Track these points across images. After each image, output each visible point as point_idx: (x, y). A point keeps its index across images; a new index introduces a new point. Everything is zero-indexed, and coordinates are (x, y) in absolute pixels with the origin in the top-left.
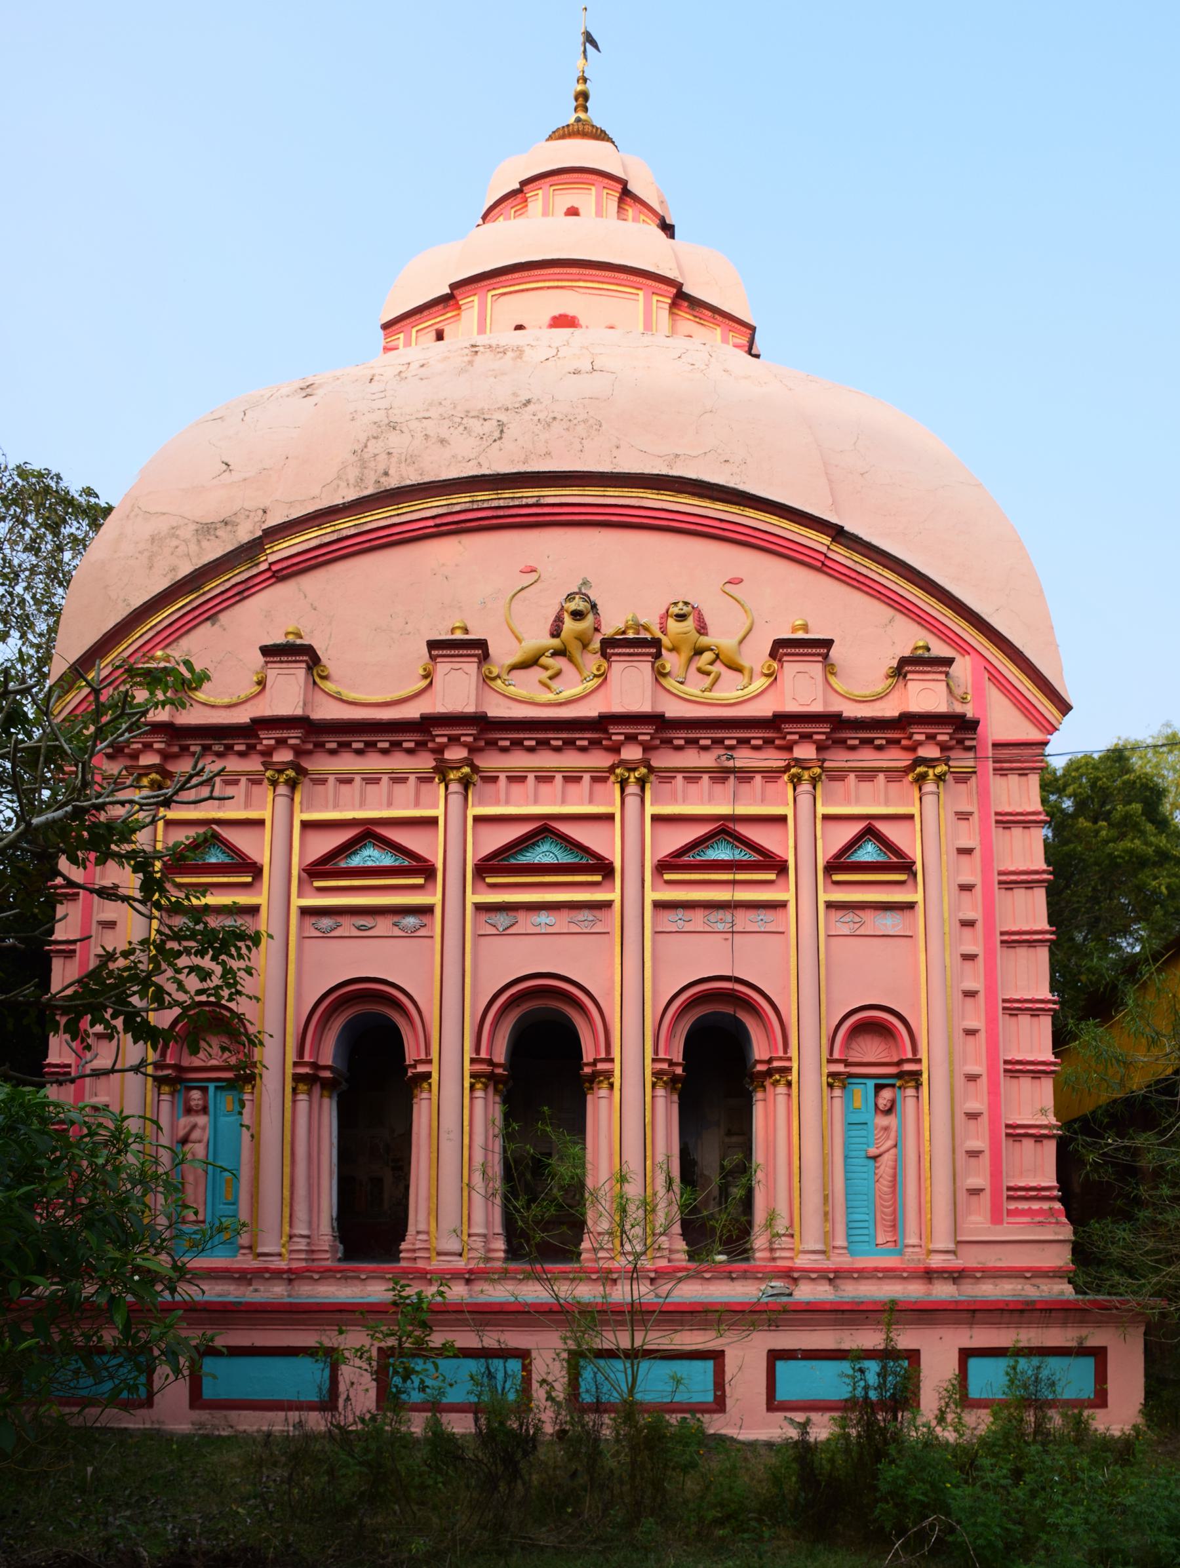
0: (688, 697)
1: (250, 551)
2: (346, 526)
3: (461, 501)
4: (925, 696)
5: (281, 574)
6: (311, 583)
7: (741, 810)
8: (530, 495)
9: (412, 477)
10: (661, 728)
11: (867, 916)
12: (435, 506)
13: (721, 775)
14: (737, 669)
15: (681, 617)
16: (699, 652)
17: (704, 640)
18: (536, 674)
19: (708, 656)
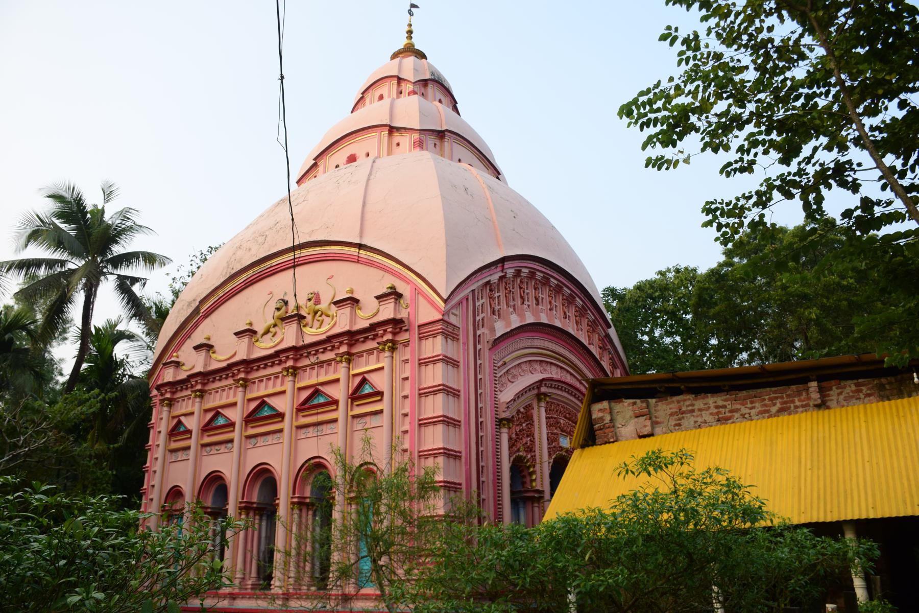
0: (313, 334)
1: (197, 311)
2: (221, 293)
3: (250, 273)
4: (387, 311)
5: (207, 315)
6: (214, 316)
7: (322, 379)
8: (269, 264)
9: (239, 267)
10: (297, 351)
11: (367, 419)
12: (244, 277)
13: (321, 364)
14: (328, 316)
15: (310, 300)
16: (316, 313)
17: (318, 307)
18: (270, 335)
19: (319, 313)
